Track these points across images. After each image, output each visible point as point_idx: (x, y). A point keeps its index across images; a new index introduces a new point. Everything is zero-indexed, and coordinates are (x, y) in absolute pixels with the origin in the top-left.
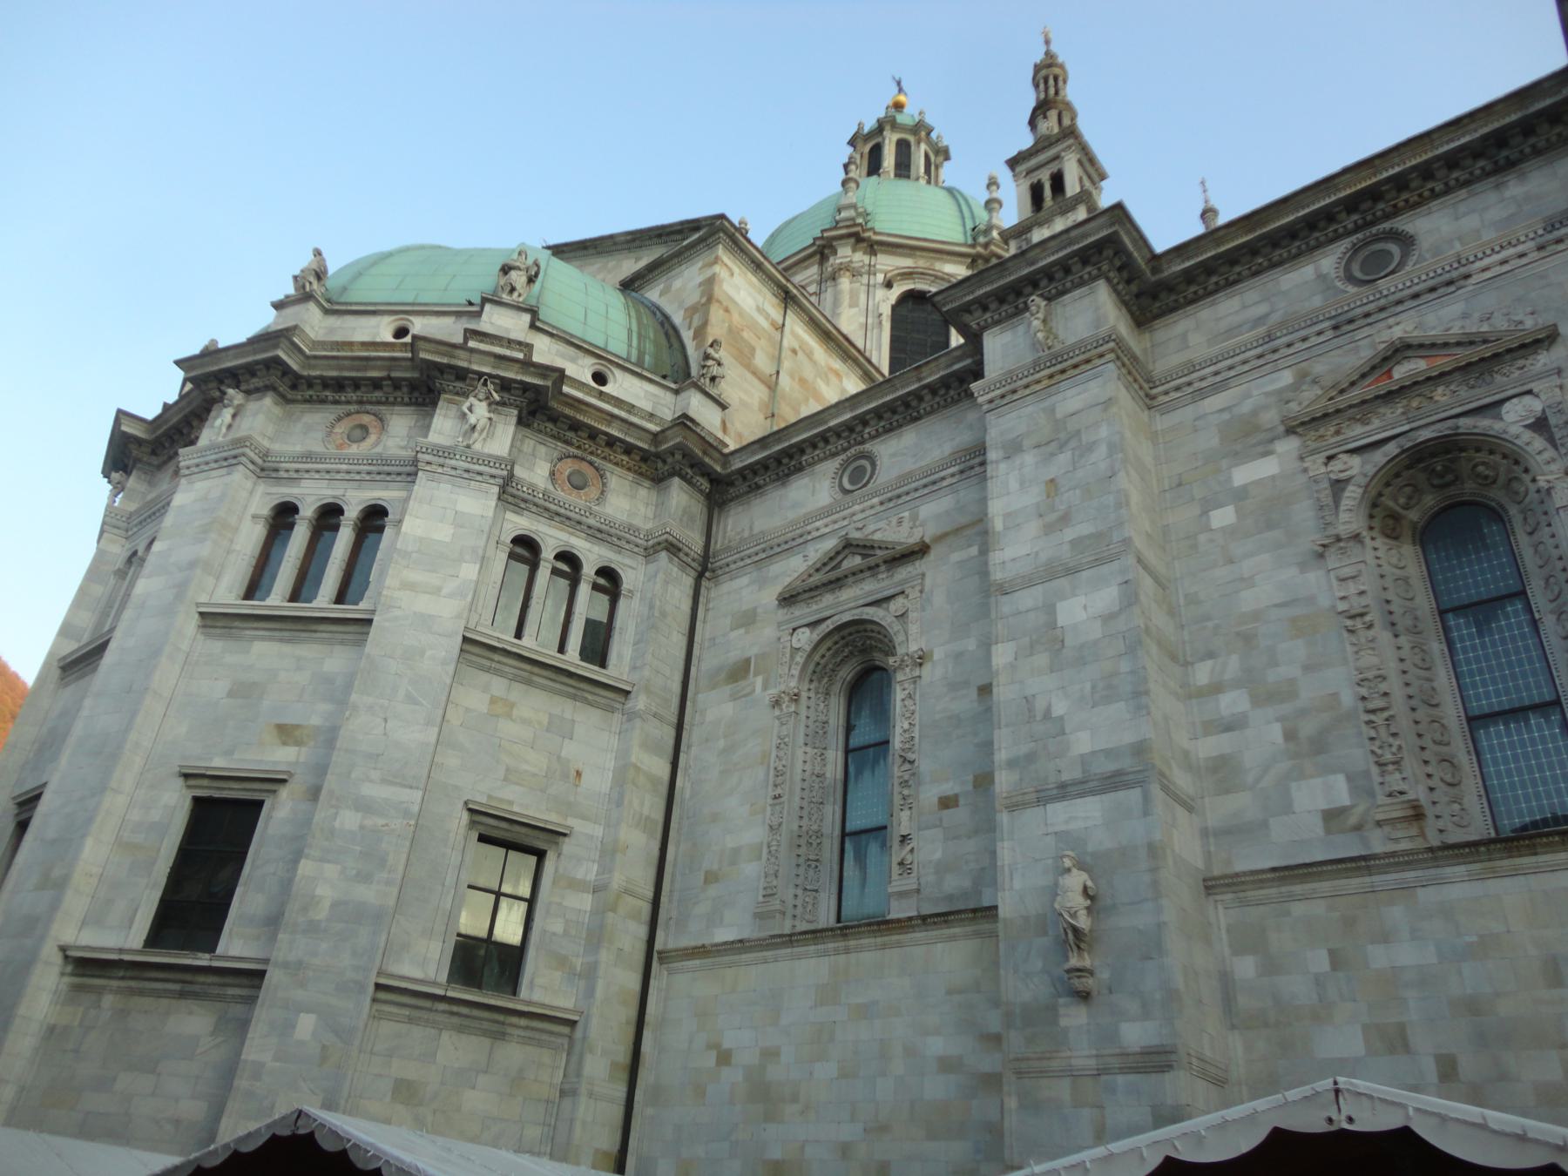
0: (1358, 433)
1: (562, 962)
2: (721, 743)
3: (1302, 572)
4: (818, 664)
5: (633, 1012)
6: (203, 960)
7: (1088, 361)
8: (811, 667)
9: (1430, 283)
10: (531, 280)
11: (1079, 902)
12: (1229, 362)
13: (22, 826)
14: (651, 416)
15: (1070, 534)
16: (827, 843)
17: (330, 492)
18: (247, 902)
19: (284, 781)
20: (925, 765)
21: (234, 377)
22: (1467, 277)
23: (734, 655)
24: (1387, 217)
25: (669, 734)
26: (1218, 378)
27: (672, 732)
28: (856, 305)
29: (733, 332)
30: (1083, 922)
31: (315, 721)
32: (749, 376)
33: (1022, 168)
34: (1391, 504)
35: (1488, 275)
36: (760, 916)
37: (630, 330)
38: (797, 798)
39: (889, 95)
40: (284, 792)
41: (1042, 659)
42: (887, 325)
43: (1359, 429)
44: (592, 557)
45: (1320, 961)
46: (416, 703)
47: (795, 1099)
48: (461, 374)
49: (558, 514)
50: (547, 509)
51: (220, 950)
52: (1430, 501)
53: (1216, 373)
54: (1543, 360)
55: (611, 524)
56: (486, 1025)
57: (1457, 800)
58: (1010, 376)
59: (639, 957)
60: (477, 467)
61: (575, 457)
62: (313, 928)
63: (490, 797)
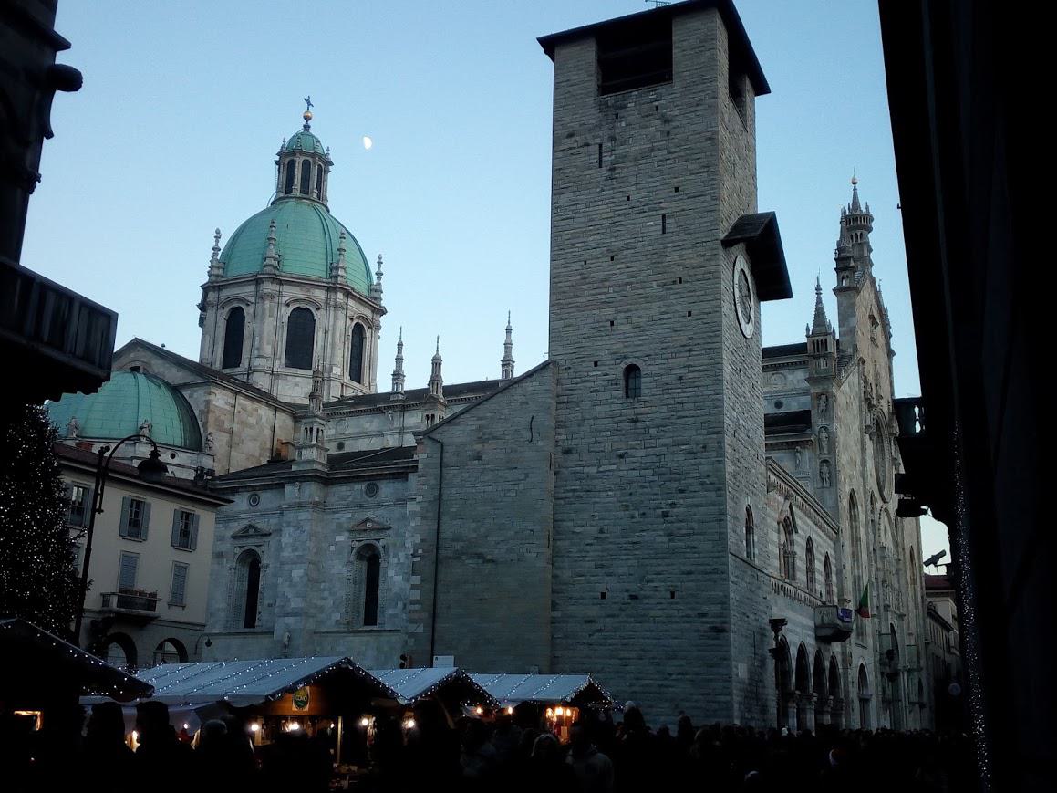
11: (286, 639)
15: (297, 554)
29: (217, 419)
30: (287, 643)
32: (222, 433)
36: (226, 627)
42: (286, 328)
45: (329, 648)
52: (370, 552)
54: (387, 532)
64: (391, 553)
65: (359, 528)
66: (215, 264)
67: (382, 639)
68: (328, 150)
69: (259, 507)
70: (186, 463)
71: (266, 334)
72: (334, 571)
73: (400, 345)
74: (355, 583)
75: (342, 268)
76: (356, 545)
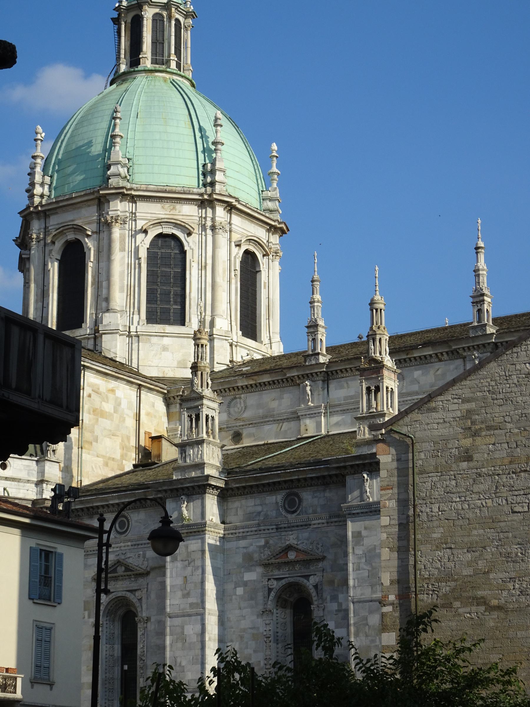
0: (277, 573)
3: (258, 618)
4: (109, 610)
7: (199, 531)
8: (107, 611)
9: (301, 523)
12: (247, 530)
14: (28, 481)
22: (310, 525)
24: (296, 488)
26: (244, 534)
34: (284, 597)
35: (315, 526)
38: (104, 666)
41: (179, 645)
42: (144, 266)
53: (243, 532)
54: (320, 565)
64: (327, 595)
69: (130, 535)
70: (23, 475)
74: (277, 641)
75: (221, 170)
76: (275, 584)
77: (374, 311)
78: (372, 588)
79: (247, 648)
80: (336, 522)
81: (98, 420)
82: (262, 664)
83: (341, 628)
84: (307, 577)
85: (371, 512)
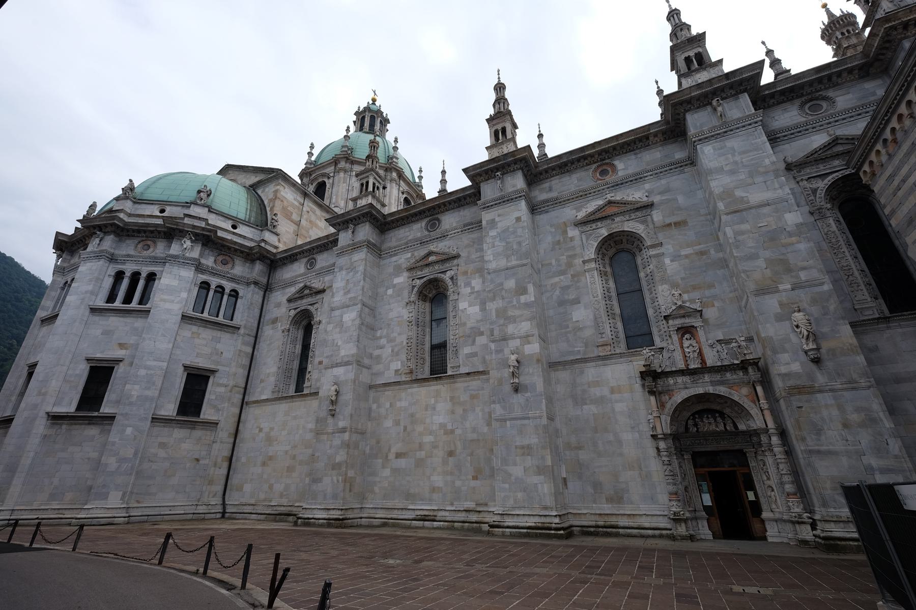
1: (215, 407)
2: (268, 342)
5: (236, 419)
6: (96, 414)
10: (209, 195)
13: (30, 375)
14: (252, 240)
15: (349, 296)
16: (294, 371)
17: (136, 268)
18: (110, 396)
19: (121, 361)
20: (317, 353)
21: (100, 228)
22: (448, 235)
23: (274, 316)
24: (437, 214)
25: (252, 339)
27: (254, 339)
28: (346, 183)
29: (284, 209)
30: (334, 398)
31: (132, 342)
33: (359, 177)
36: (273, 392)
37: (247, 209)
39: (372, 95)
40: (121, 364)
41: (338, 330)
43: (420, 273)
44: (229, 287)
45: (388, 405)
46: (165, 336)
47: (277, 441)
48: (181, 231)
49: (217, 274)
50: (212, 273)
51: (101, 411)
52: (434, 292)
54: (455, 262)
55: (235, 276)
56: (189, 426)
57: (423, 368)
58: (343, 247)
59: (240, 404)
60: (187, 261)
61: (223, 254)
62: (131, 404)
63: (191, 362)
65: (424, 263)
66: (309, 161)
67: (458, 385)
68: (387, 115)
70: (249, 235)
71: (340, 193)
72: (392, 315)
73: (444, 172)
76: (418, 283)
77: (498, 89)
78: (507, 259)
79: (393, 332)
80: (469, 229)
81: (312, 228)
82: (405, 343)
83: (474, 306)
84: (444, 272)
85: (504, 202)
